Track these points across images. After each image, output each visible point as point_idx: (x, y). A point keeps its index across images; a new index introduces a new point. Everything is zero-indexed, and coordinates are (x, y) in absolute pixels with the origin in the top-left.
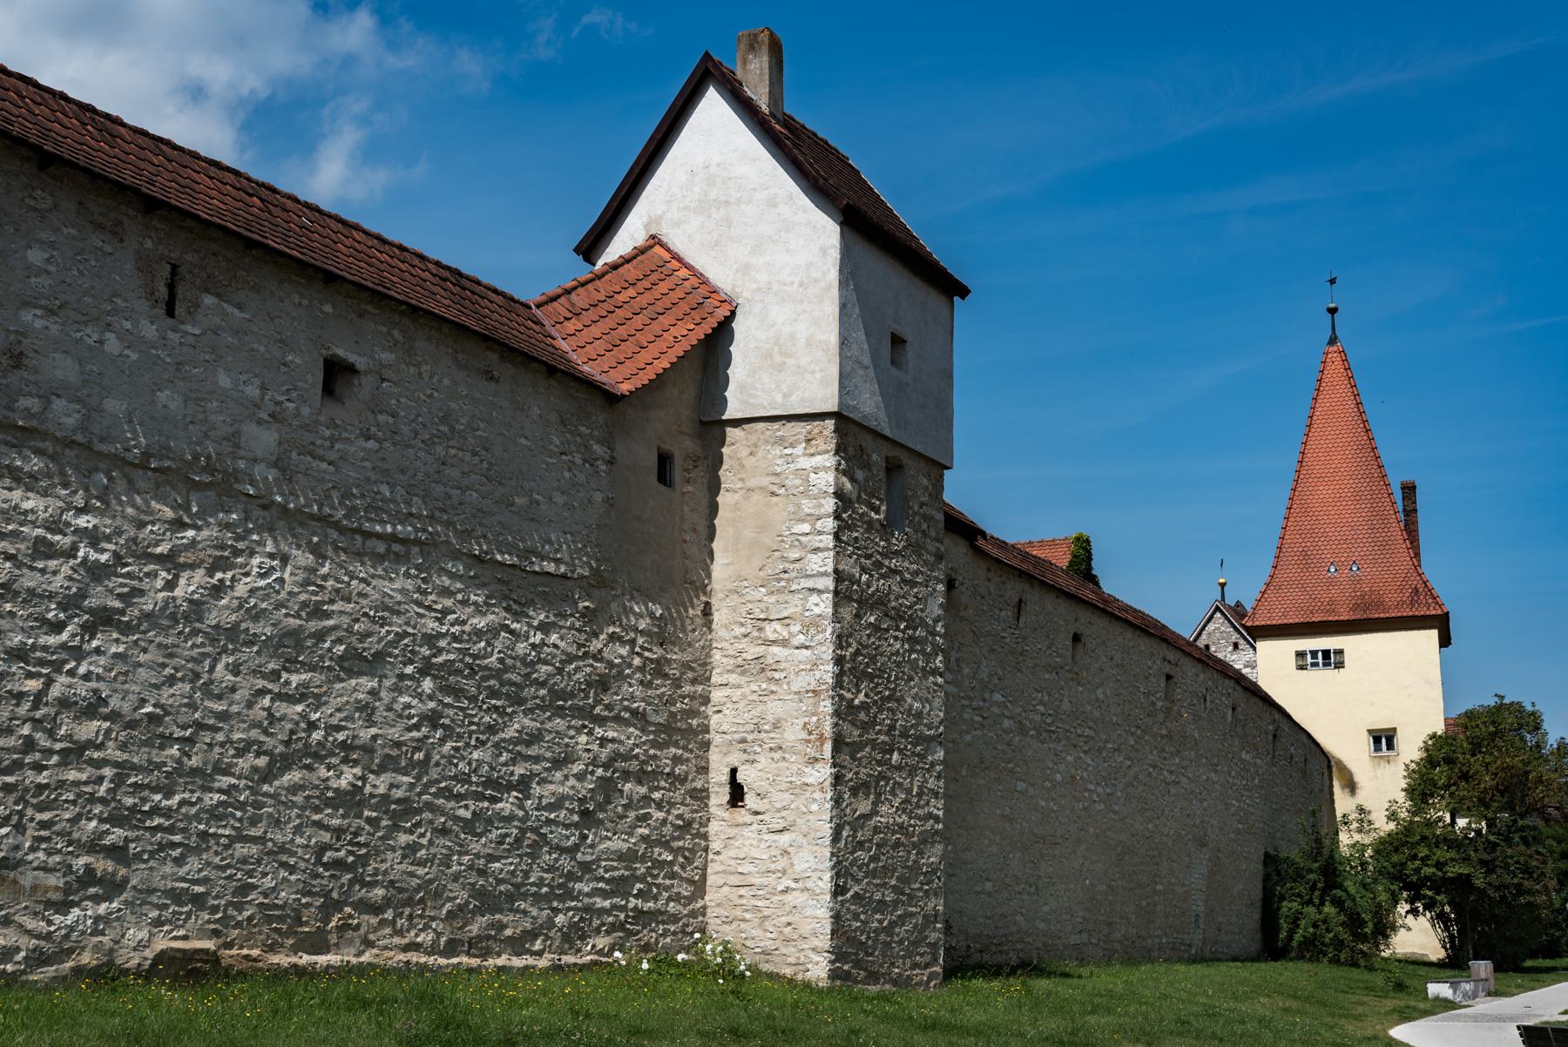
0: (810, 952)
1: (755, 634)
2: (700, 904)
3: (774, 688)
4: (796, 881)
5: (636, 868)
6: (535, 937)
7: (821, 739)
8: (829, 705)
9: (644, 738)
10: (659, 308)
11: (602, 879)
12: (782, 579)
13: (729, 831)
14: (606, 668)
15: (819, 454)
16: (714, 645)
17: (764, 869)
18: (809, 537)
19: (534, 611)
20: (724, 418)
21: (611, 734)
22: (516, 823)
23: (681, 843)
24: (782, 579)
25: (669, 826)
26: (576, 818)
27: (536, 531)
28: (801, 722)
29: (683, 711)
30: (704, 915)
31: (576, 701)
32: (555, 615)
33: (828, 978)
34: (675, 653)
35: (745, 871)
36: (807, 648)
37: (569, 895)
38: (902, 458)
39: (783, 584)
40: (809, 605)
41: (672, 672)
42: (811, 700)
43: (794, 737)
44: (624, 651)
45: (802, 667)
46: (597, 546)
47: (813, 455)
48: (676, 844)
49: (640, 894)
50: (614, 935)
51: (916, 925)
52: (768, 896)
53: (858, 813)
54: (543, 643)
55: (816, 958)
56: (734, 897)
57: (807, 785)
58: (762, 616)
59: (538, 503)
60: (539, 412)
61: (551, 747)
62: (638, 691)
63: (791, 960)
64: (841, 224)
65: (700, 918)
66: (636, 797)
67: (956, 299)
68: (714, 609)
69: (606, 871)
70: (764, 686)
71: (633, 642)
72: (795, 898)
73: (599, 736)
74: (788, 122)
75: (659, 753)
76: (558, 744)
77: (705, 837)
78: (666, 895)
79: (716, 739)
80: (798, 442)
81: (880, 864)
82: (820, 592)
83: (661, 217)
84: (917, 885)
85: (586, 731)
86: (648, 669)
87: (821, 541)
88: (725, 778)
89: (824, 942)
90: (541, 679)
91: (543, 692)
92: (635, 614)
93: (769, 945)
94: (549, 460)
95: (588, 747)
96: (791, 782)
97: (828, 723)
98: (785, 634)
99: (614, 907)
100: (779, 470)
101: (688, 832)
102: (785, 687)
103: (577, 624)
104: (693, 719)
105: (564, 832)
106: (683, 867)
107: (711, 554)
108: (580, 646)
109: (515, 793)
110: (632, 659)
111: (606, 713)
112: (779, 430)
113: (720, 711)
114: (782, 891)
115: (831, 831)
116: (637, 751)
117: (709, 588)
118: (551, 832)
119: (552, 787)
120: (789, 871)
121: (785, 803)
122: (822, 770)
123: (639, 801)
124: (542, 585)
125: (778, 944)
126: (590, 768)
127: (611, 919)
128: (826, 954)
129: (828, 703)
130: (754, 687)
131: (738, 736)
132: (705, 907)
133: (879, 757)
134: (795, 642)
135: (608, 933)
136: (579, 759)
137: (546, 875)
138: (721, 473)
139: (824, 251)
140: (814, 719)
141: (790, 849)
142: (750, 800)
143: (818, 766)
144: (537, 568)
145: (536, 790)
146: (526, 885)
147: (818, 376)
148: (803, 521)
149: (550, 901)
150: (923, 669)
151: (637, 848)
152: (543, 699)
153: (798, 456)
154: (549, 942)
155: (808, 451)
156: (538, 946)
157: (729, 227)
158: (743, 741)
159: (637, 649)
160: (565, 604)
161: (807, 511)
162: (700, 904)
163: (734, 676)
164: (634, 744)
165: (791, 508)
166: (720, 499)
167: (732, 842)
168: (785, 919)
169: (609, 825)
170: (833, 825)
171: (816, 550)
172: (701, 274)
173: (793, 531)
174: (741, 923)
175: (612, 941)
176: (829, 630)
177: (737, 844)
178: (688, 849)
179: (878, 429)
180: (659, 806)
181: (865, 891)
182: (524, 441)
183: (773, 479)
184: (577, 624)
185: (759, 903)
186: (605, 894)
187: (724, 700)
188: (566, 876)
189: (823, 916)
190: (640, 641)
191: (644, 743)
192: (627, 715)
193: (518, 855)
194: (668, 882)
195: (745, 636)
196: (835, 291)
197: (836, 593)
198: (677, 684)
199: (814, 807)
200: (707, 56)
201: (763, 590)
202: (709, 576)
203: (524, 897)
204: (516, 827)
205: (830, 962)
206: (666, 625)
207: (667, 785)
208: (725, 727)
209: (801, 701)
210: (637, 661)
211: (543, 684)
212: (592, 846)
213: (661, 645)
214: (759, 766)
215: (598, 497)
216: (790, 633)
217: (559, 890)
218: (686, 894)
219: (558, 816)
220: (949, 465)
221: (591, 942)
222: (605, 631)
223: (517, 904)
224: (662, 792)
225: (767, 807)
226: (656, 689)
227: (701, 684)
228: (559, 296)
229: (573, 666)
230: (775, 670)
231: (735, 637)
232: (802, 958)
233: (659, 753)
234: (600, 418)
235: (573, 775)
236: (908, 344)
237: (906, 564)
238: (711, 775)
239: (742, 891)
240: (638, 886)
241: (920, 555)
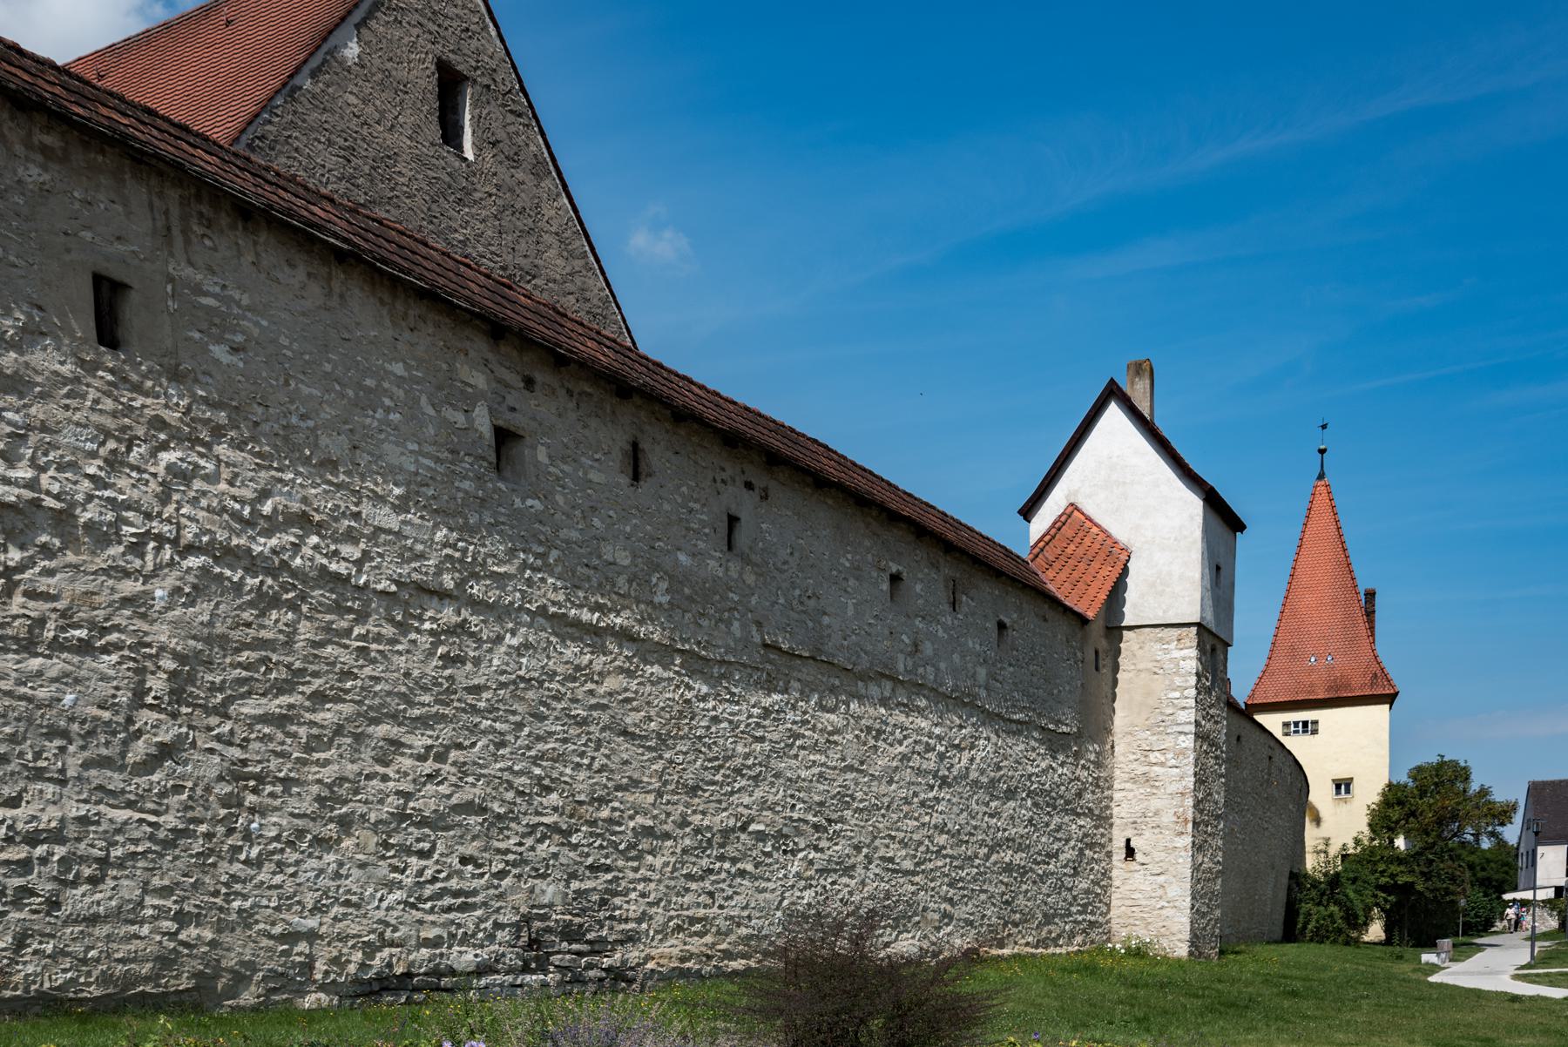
7: (1186, 821)
55: (1180, 945)
79: (1116, 821)
80: (1172, 641)
82: (1186, 734)
88: (1123, 844)
130: (1142, 791)
134: (1169, 764)
139: (1192, 518)
142: (1139, 856)
148: (1175, 690)
158: (1135, 822)
165: (1167, 682)
171: (1184, 708)
199: (1181, 860)
208: (1123, 815)
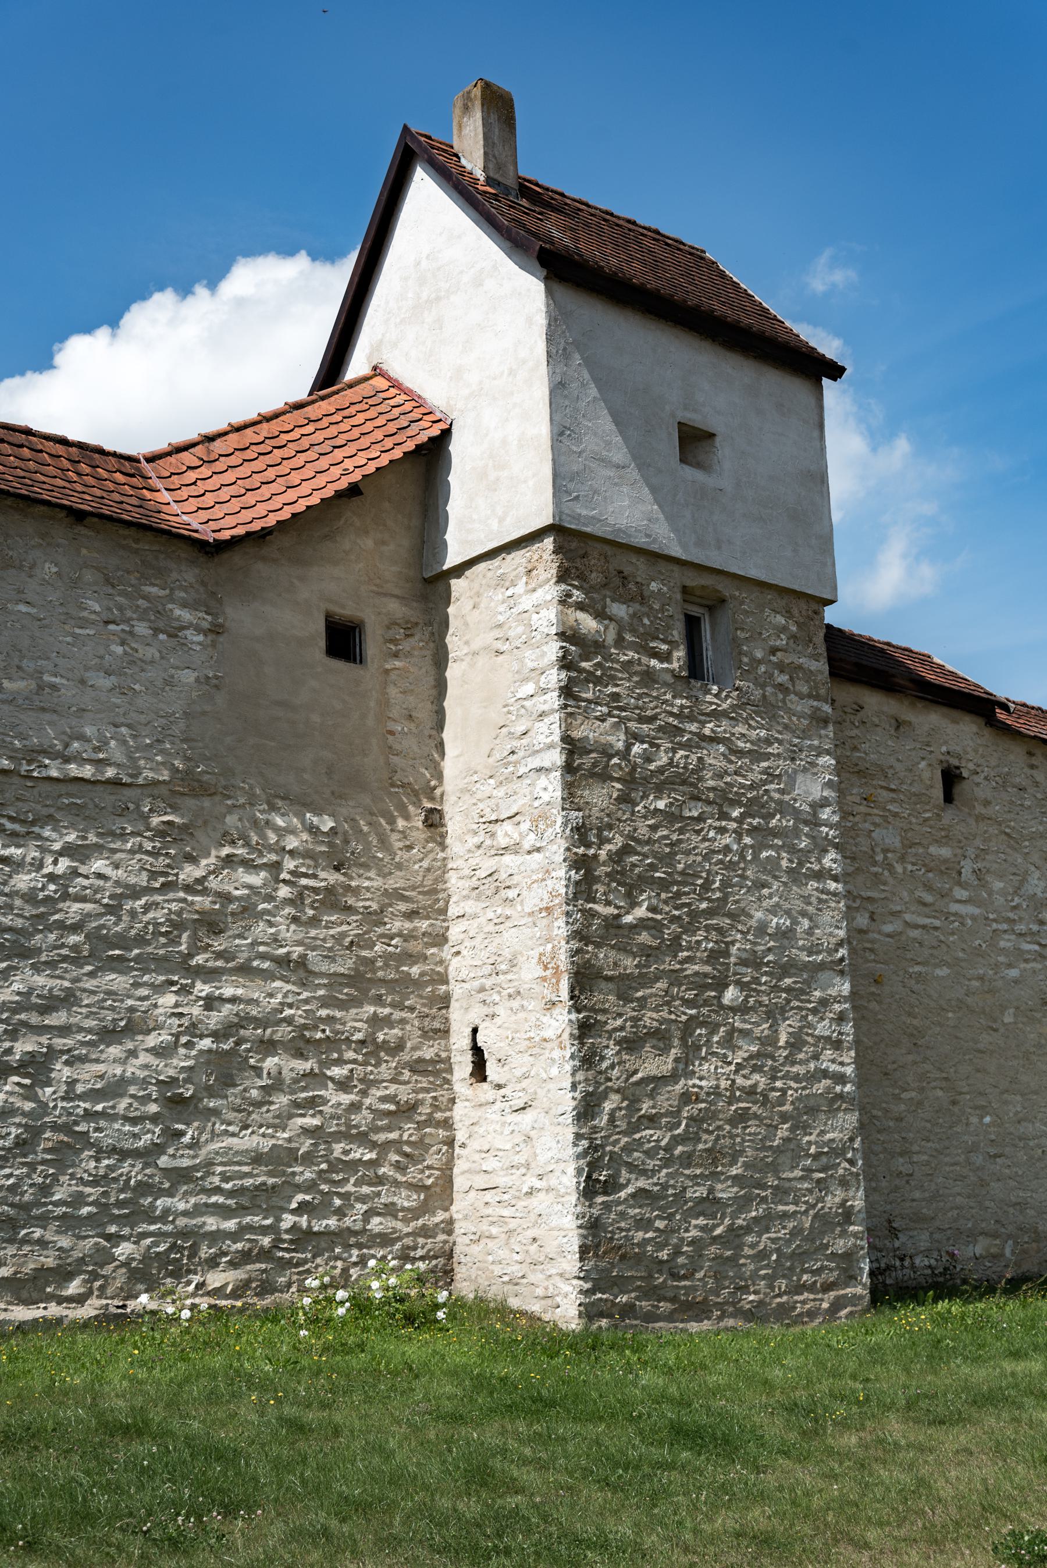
0: (558, 1278)
1: (488, 842)
2: (440, 1216)
3: (508, 912)
4: (540, 1177)
5: (294, 1174)
6: (70, 1276)
7: (557, 972)
8: (563, 925)
9: (305, 995)
10: (338, 442)
11: (218, 1190)
12: (509, 763)
13: (473, 1114)
14: (215, 903)
15: (541, 586)
16: (450, 866)
17: (507, 1164)
18: (534, 699)
19: (54, 830)
20: (445, 568)
21: (228, 992)
22: (17, 1120)
23: (393, 1136)
24: (509, 763)
25: (364, 1112)
26: (153, 1108)
27: (49, 723)
28: (535, 954)
29: (387, 957)
30: (450, 1232)
31: (150, 949)
32: (99, 835)
33: (580, 1316)
34: (369, 879)
35: (489, 1169)
36: (538, 850)
37: (139, 1214)
38: (720, 587)
39: (511, 769)
40: (538, 791)
41: (361, 904)
42: (545, 922)
43: (530, 976)
44: (256, 879)
45: (535, 877)
46: (184, 741)
47: (534, 590)
48: (381, 1137)
49: (303, 1208)
50: (249, 1267)
51: (795, 1233)
52: (513, 1202)
53: (640, 1075)
54: (75, 873)
55: (566, 1288)
56: (480, 1204)
57: (545, 1040)
58: (493, 818)
59: (54, 687)
60: (54, 570)
61: (96, 1013)
62: (289, 932)
63: (540, 1292)
64: (546, 280)
65: (442, 1237)
66: (287, 1075)
67: (825, 381)
68: (447, 817)
69: (225, 1178)
70: (499, 911)
71: (277, 866)
72: (540, 1202)
73: (203, 994)
74: (526, 189)
75: (338, 1014)
76: (112, 1008)
77: (447, 1124)
78: (361, 1208)
79: (457, 990)
80: (518, 577)
81: (701, 1146)
82: (548, 770)
83: (381, 341)
84: (798, 1173)
85: (174, 989)
86: (308, 901)
87: (545, 702)
88: (466, 1042)
89: (571, 1264)
90: (69, 922)
91: (73, 939)
92: (277, 829)
93: (516, 1270)
94: (78, 631)
95: (180, 1010)
96: (529, 1039)
97: (563, 950)
98: (516, 836)
99: (243, 1229)
100: (501, 618)
101: (410, 1119)
102: (519, 908)
103: (148, 846)
104: (411, 966)
105: (127, 1128)
106: (398, 1167)
107: (440, 746)
108: (153, 875)
109: (16, 1079)
110: (276, 890)
111: (220, 963)
112: (500, 567)
113: (458, 953)
114: (527, 1193)
115: (574, 1103)
116: (288, 1012)
117: (438, 792)
118: (97, 1130)
119: (101, 1068)
120: (533, 1165)
121: (525, 1069)
122: (560, 1017)
123: (295, 1081)
124: (69, 795)
125: (524, 1269)
126: (184, 1040)
127: (239, 1246)
128: (575, 1282)
129: (561, 922)
130: (490, 915)
131: (476, 984)
132: (451, 1222)
133: (690, 995)
134: (527, 845)
135: (233, 1265)
136: (158, 1027)
137: (88, 1190)
138: (448, 639)
139: (529, 321)
140: (549, 946)
141: (532, 1134)
142: (492, 1069)
143: (556, 1011)
144: (54, 773)
145: (62, 1072)
146: (45, 1204)
147: (531, 483)
148: (526, 680)
149: (103, 1225)
150: (790, 871)
151: (293, 1145)
152: (75, 948)
153: (520, 596)
154: (97, 1284)
155: (530, 587)
156: (74, 1287)
157: (441, 328)
158: (482, 990)
159: (284, 876)
160: (122, 819)
161: (531, 665)
162: (440, 1216)
163: (470, 902)
164: (281, 1003)
165: (516, 667)
166: (448, 674)
167: (476, 1128)
168: (531, 1233)
169: (231, 1116)
170: (577, 1095)
171: (542, 715)
172: (419, 397)
173: (519, 696)
174: (488, 1241)
175: (244, 1276)
176: (560, 820)
177: (481, 1131)
178: (408, 1143)
179: (654, 547)
180: (344, 1085)
181: (665, 1187)
182: (23, 608)
183: (498, 633)
184: (148, 846)
185: (506, 1212)
186: (225, 1212)
187: (462, 936)
188: (134, 1189)
189: (567, 1226)
190: (290, 864)
191: (306, 1001)
192: (266, 965)
193: (24, 1164)
194: (366, 1190)
195: (479, 847)
196: (543, 369)
197: (569, 768)
198: (375, 918)
199: (554, 1071)
200: (406, 129)
201: (492, 781)
202: (440, 777)
203: (43, 1221)
204: (19, 1125)
205: (581, 1292)
206: (346, 842)
207: (360, 1058)
208: (463, 975)
209: (535, 925)
210: (284, 892)
211: (76, 928)
212: (194, 1145)
213: (337, 869)
214: (498, 1021)
215: (188, 677)
216: (520, 834)
217: (119, 1208)
218: (406, 1204)
219: (113, 1107)
220: (827, 596)
221: (196, 1279)
222: (213, 853)
223: (23, 1232)
224: (350, 1066)
225: (509, 1076)
226: (327, 927)
227: (428, 918)
228: (193, 445)
229: (143, 902)
230: (509, 887)
231: (469, 851)
232: (551, 1287)
233: (338, 1014)
234: (189, 575)
235: (147, 1050)
236: (718, 440)
237: (741, 729)
238: (452, 1041)
239: (488, 1196)
240: (300, 1197)
241: (774, 717)
